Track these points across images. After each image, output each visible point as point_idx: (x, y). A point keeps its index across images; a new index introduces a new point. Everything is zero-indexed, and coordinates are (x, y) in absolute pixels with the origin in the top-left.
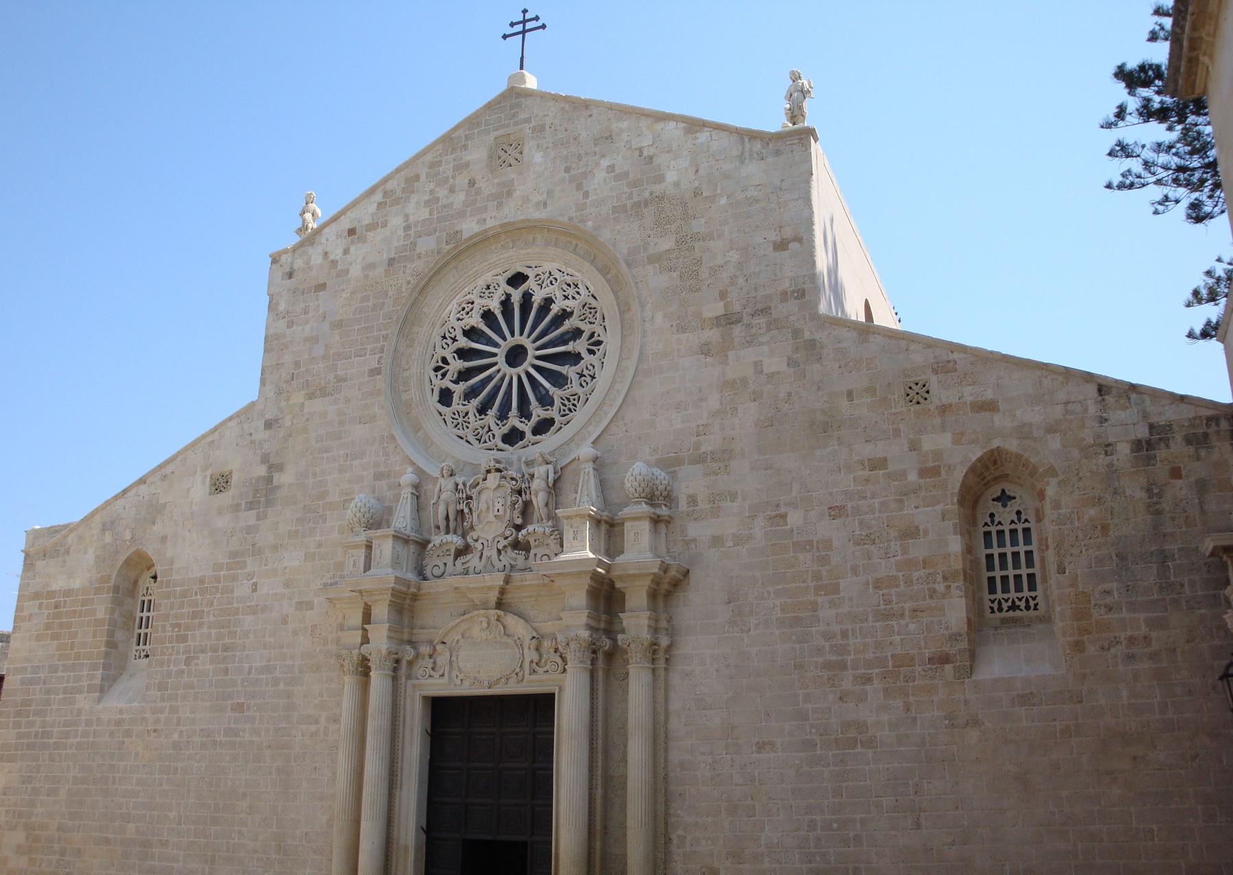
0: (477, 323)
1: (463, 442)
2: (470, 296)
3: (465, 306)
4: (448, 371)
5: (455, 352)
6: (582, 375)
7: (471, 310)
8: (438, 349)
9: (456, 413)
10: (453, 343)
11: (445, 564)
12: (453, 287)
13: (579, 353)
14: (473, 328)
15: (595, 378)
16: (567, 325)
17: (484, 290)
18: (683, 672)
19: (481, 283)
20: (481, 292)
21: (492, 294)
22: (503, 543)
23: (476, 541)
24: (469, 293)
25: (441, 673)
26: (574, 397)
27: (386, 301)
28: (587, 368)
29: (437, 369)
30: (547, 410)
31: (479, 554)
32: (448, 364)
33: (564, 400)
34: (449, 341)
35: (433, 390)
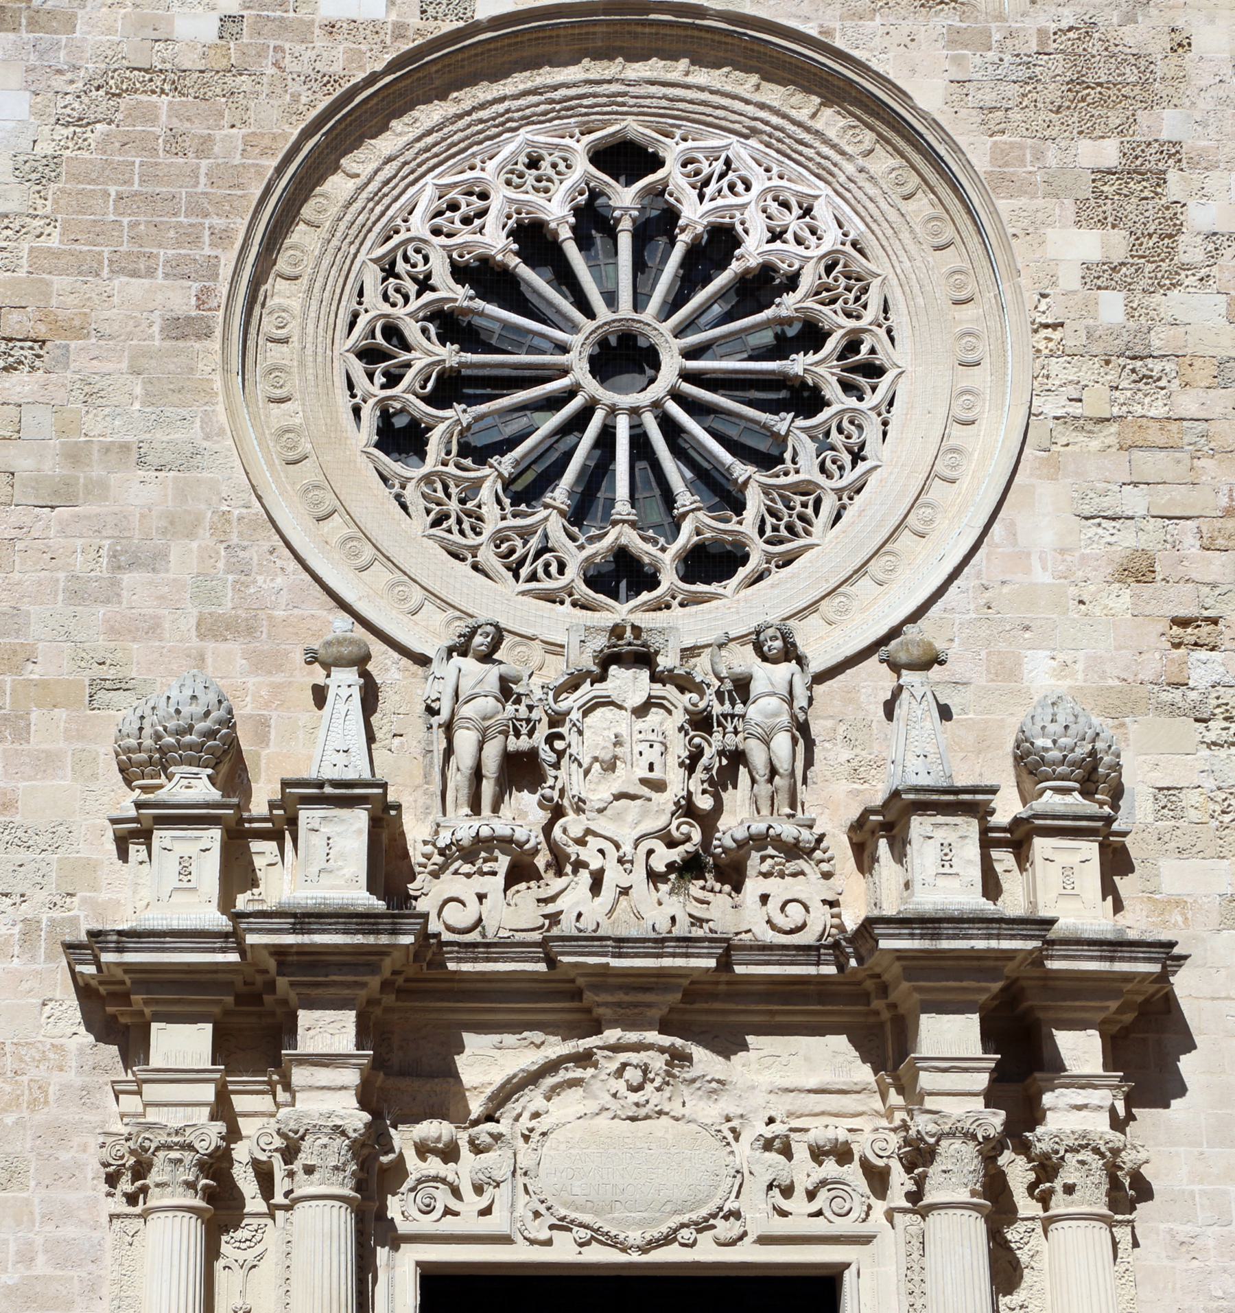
0: (504, 250)
1: (465, 568)
2: (469, 175)
3: (462, 200)
4: (408, 365)
5: (425, 319)
6: (824, 445)
7: (482, 213)
8: (372, 295)
9: (439, 486)
10: (419, 295)
11: (481, 897)
12: (429, 140)
13: (816, 390)
14: (485, 260)
15: (864, 459)
16: (788, 304)
17: (520, 167)
18: (1173, 1237)
19: (513, 146)
20: (512, 172)
21: (544, 183)
22: (663, 857)
23: (581, 842)
24: (472, 168)
25: (483, 1202)
26: (804, 498)
27: (218, 134)
28: (840, 430)
29: (369, 355)
30: (727, 521)
31: (585, 877)
32: (407, 348)
33: (773, 500)
34: (412, 288)
35: (357, 411)
